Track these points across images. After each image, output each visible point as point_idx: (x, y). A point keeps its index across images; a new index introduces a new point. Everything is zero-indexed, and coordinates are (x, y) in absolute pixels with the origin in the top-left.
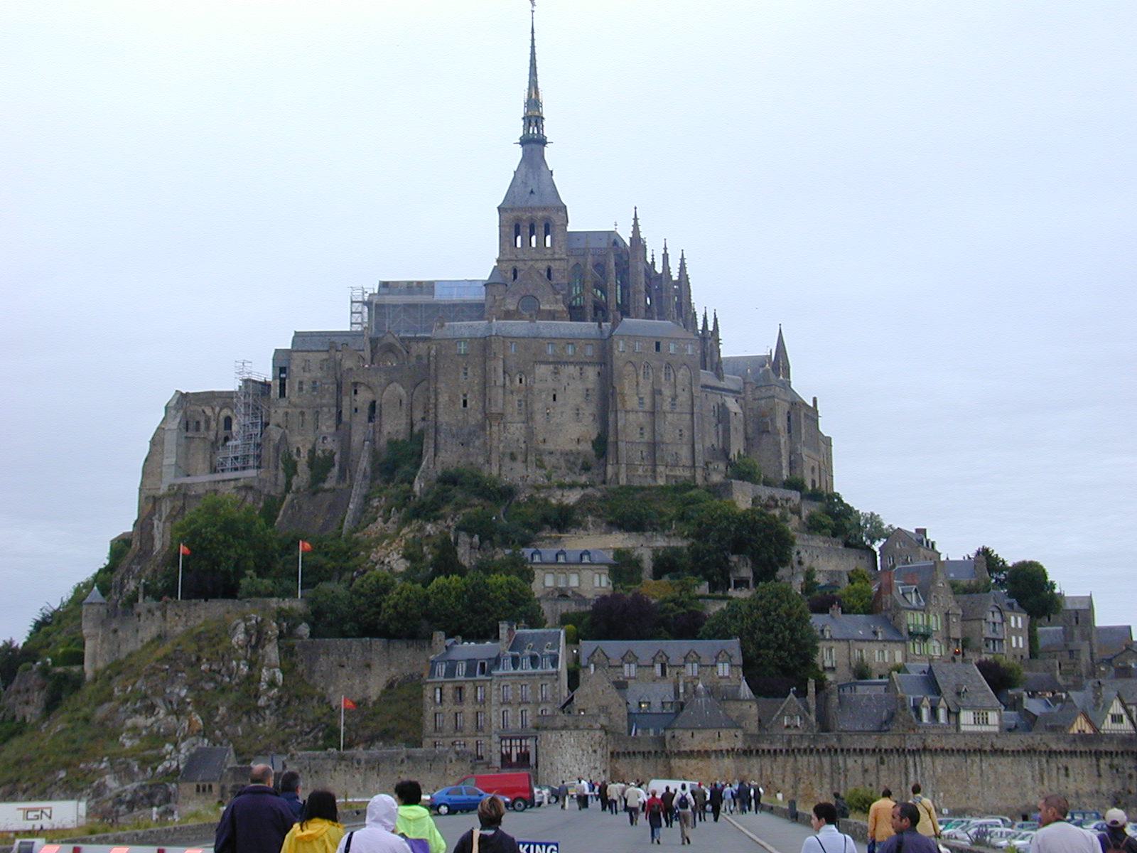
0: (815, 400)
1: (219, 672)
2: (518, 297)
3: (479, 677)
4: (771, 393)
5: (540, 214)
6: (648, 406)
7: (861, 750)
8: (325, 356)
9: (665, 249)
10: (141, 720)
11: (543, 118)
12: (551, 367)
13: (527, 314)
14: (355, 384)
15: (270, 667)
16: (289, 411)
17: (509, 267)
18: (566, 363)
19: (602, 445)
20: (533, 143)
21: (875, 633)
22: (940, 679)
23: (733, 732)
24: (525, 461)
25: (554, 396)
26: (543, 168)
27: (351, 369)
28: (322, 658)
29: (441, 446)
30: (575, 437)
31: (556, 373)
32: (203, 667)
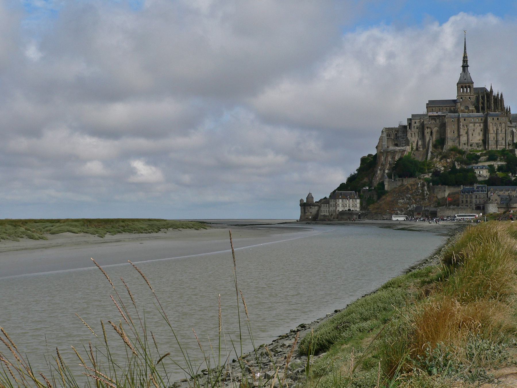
1: (416, 192)
2: (464, 106)
3: (470, 194)
5: (467, 85)
9: (498, 93)
10: (401, 201)
12: (473, 124)
13: (467, 111)
14: (427, 127)
15: (426, 191)
17: (460, 97)
19: (485, 141)
20: (465, 67)
24: (468, 145)
27: (426, 124)
28: (436, 189)
30: (479, 139)
31: (474, 125)
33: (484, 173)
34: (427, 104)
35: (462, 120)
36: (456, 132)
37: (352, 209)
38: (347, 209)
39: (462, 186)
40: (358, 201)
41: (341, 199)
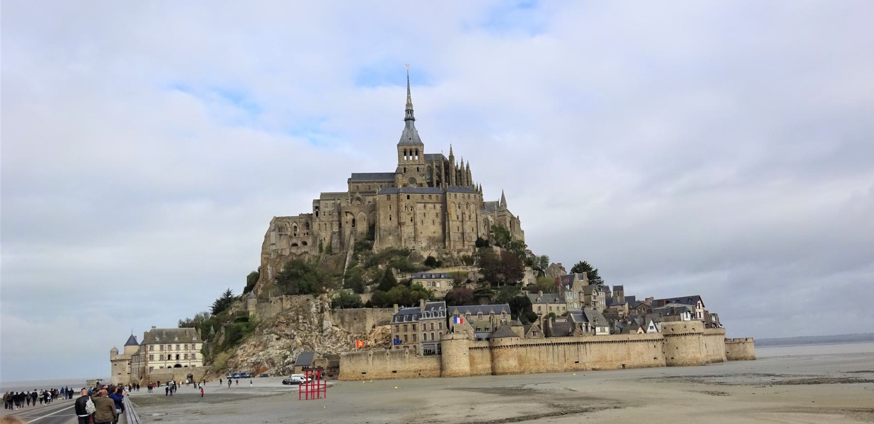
0: (518, 217)
2: (408, 179)
4: (504, 214)
6: (460, 219)
7: (564, 343)
8: (333, 202)
9: (462, 160)
11: (413, 111)
12: (423, 204)
14: (346, 212)
16: (320, 223)
17: (402, 167)
18: (428, 203)
20: (409, 119)
21: (555, 300)
22: (587, 316)
23: (516, 338)
25: (425, 215)
26: (414, 130)
27: (344, 207)
29: (382, 235)
30: (433, 231)
31: (425, 207)
32: (301, 321)
33: (442, 287)
34: (349, 179)
35: (404, 196)
36: (394, 219)
37: (183, 365)
38: (173, 363)
39: (396, 306)
40: (199, 346)
41: (157, 344)
